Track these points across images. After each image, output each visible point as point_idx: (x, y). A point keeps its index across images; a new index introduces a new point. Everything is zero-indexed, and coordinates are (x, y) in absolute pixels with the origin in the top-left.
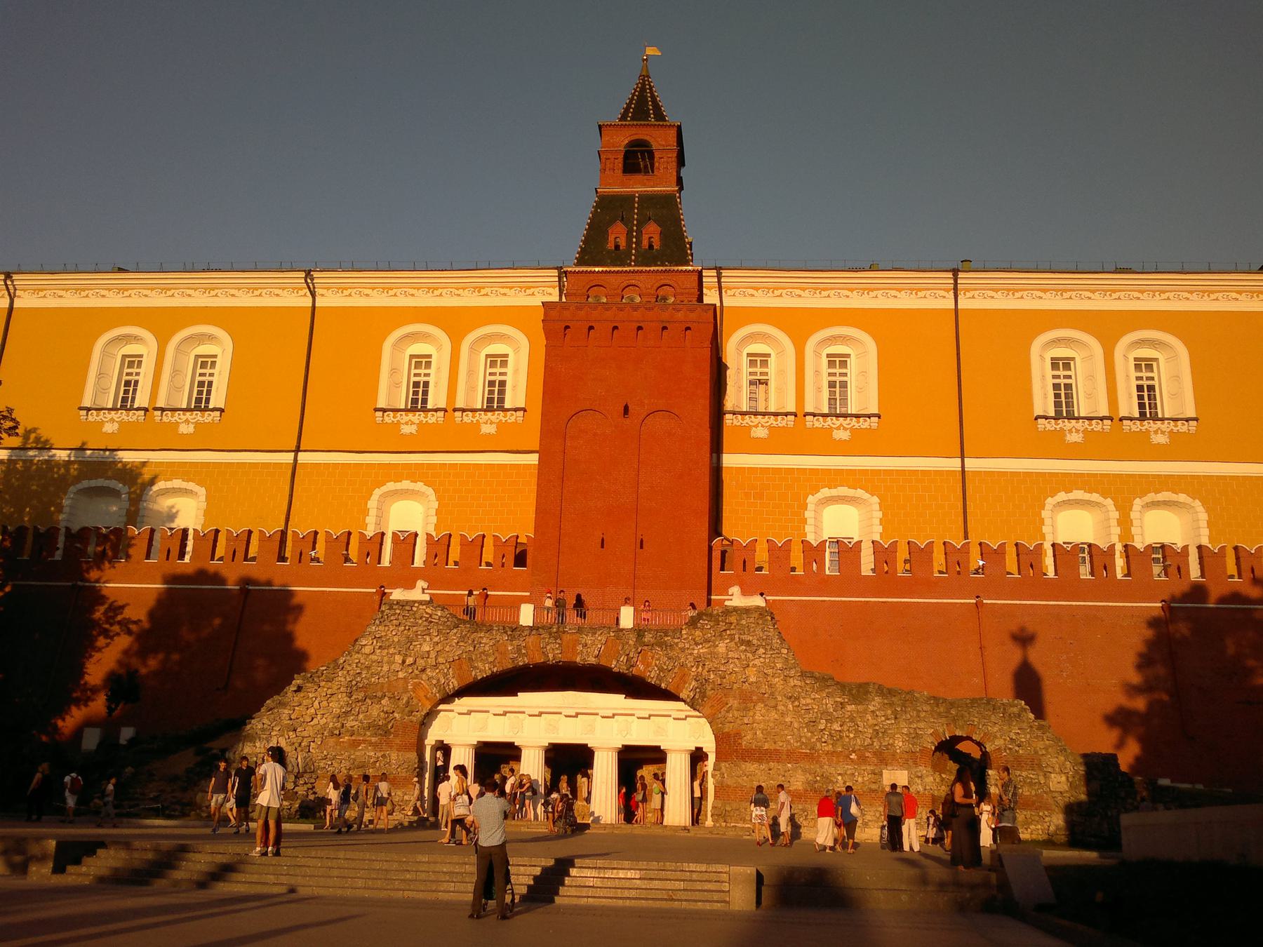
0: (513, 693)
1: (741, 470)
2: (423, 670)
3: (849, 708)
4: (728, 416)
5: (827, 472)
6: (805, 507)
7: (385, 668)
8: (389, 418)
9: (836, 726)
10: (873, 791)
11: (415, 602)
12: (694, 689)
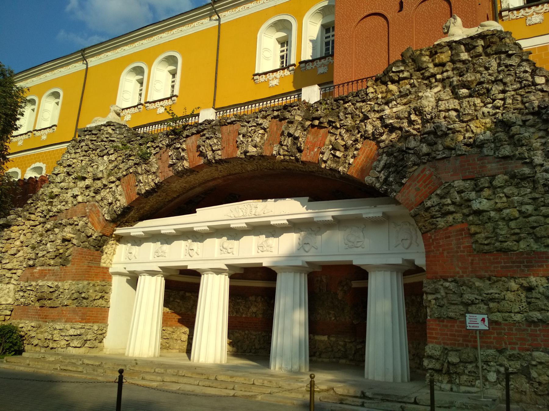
0: (193, 211)
2: (97, 192)
8: (262, 78)
12: (386, 167)
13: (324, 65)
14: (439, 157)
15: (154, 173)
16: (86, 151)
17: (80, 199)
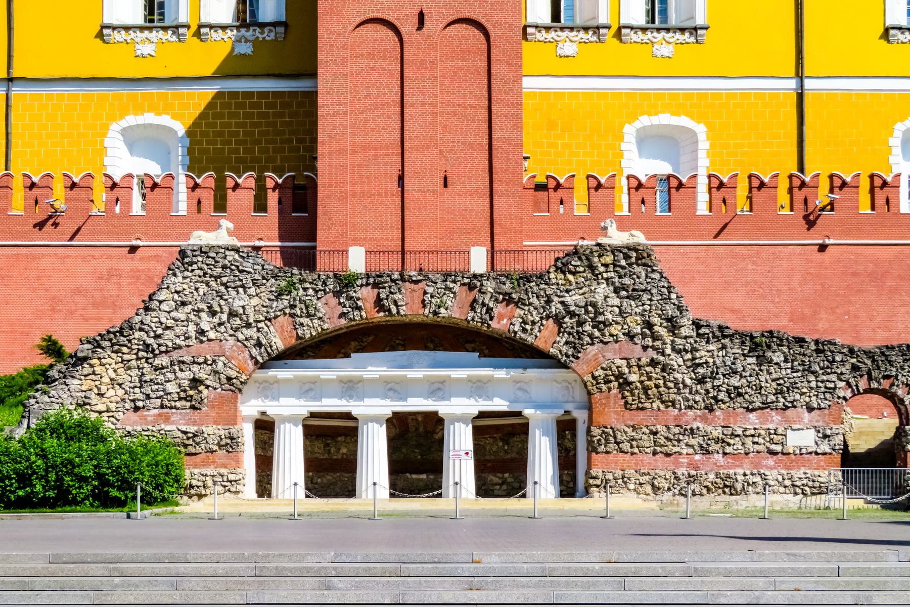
1: (545, 95)
3: (750, 360)
4: (529, 30)
5: (645, 94)
6: (621, 139)
7: (192, 329)
9: (735, 381)
13: (247, 41)
15: (320, 318)
16: (200, 277)
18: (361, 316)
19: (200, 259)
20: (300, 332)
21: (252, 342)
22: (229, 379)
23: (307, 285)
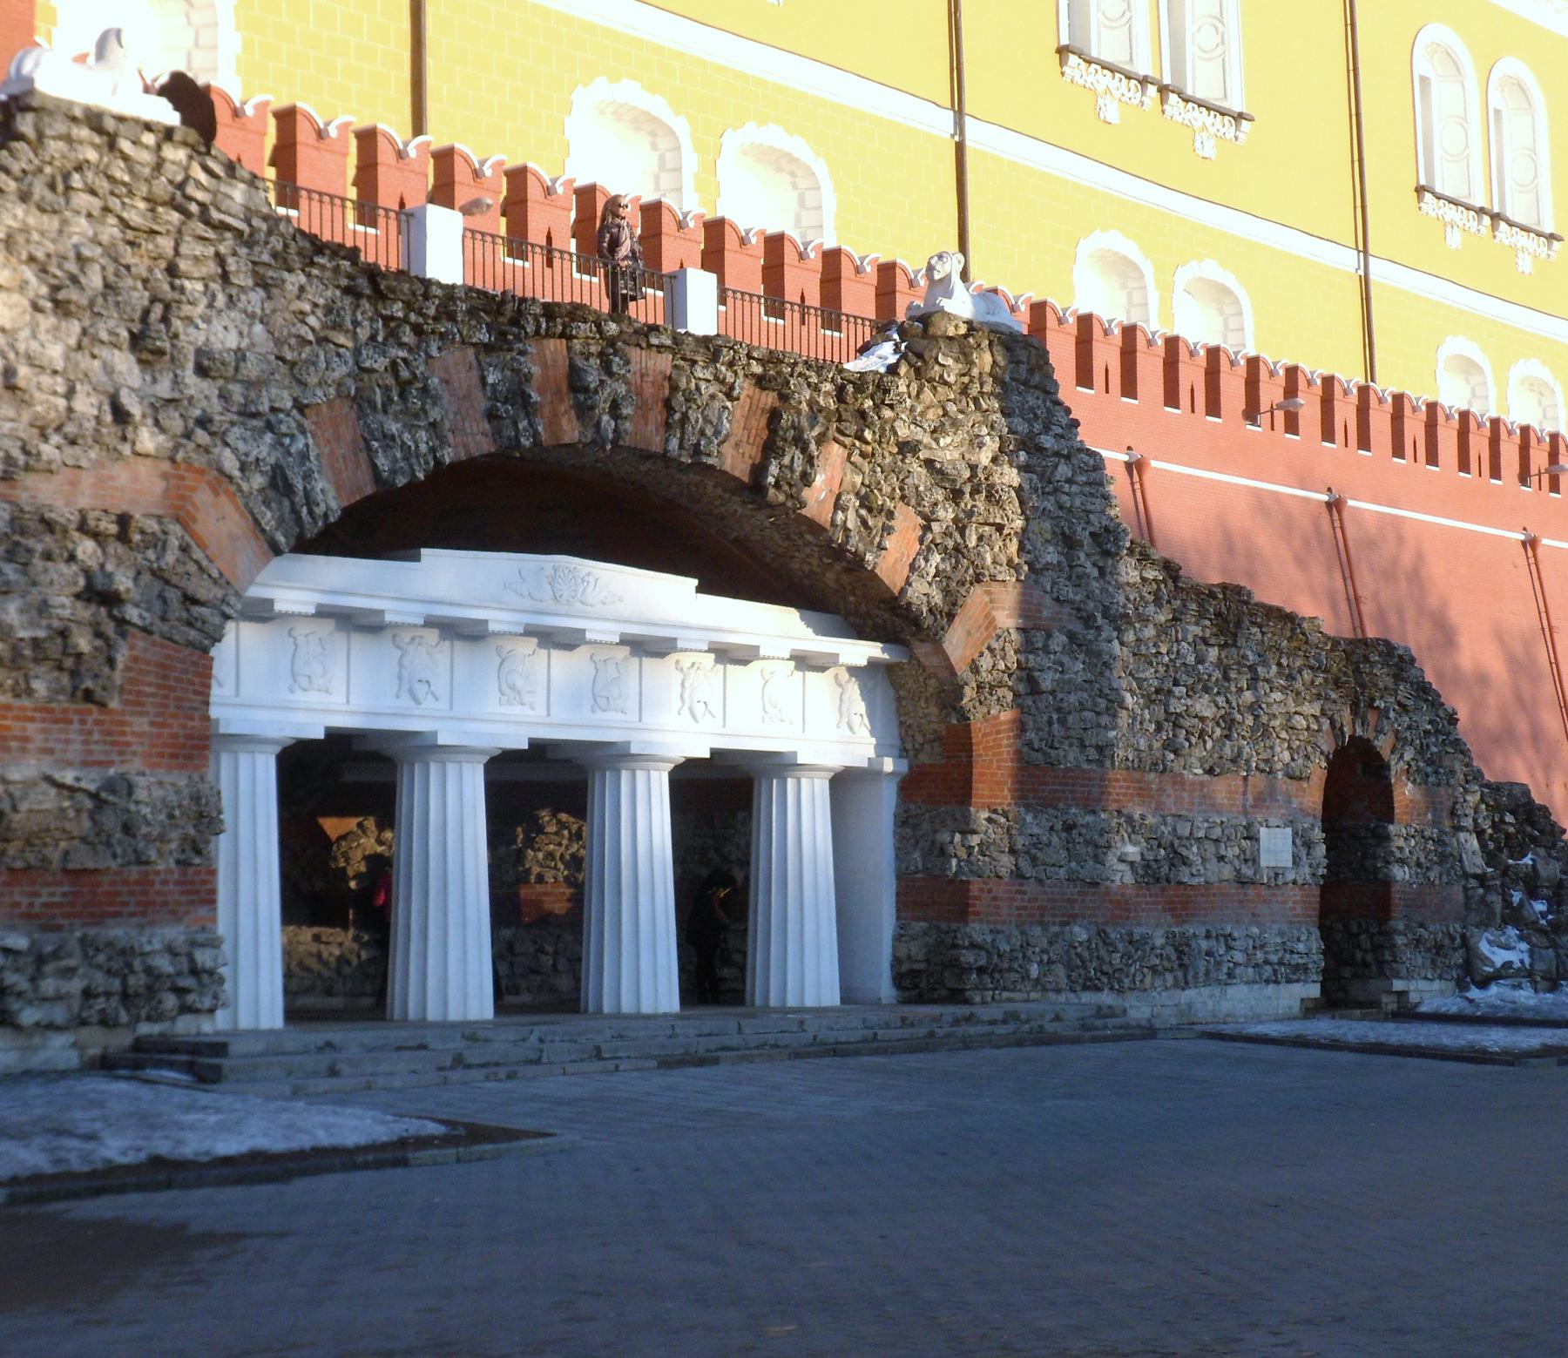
9: (1203, 706)
10: (1242, 882)
11: (148, 127)
14: (1000, 578)
15: (433, 425)
17: (148, 439)
18: (536, 434)
19: (92, 155)
20: (382, 462)
21: (258, 481)
22: (190, 600)
23: (397, 310)
